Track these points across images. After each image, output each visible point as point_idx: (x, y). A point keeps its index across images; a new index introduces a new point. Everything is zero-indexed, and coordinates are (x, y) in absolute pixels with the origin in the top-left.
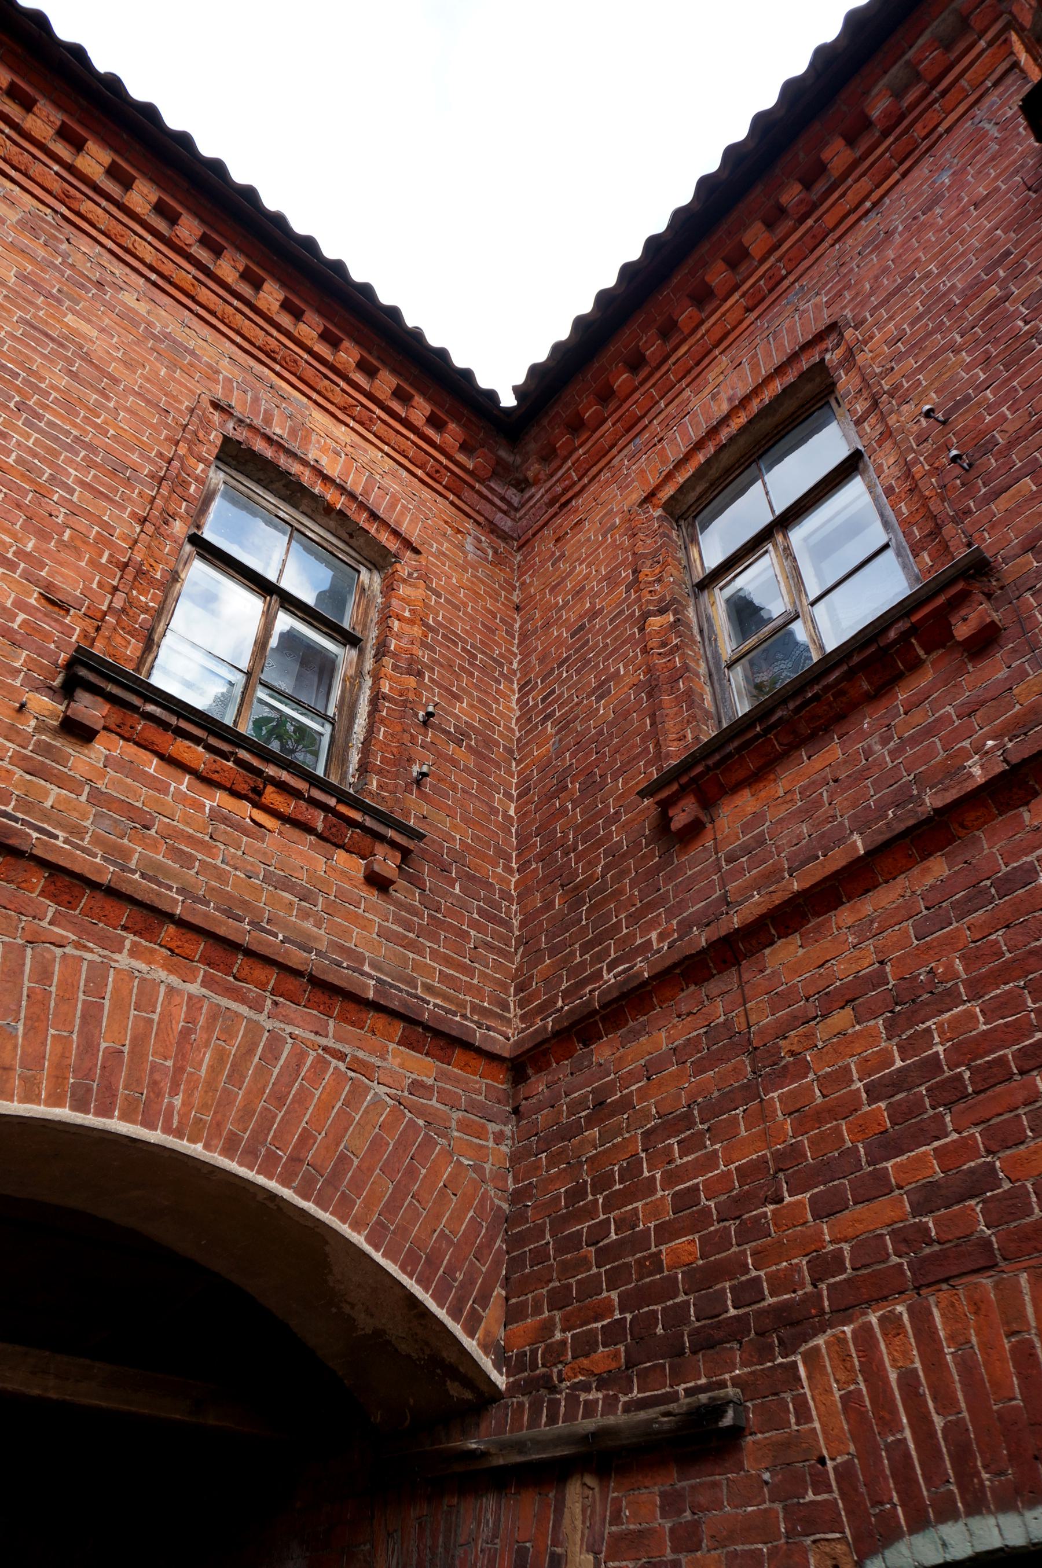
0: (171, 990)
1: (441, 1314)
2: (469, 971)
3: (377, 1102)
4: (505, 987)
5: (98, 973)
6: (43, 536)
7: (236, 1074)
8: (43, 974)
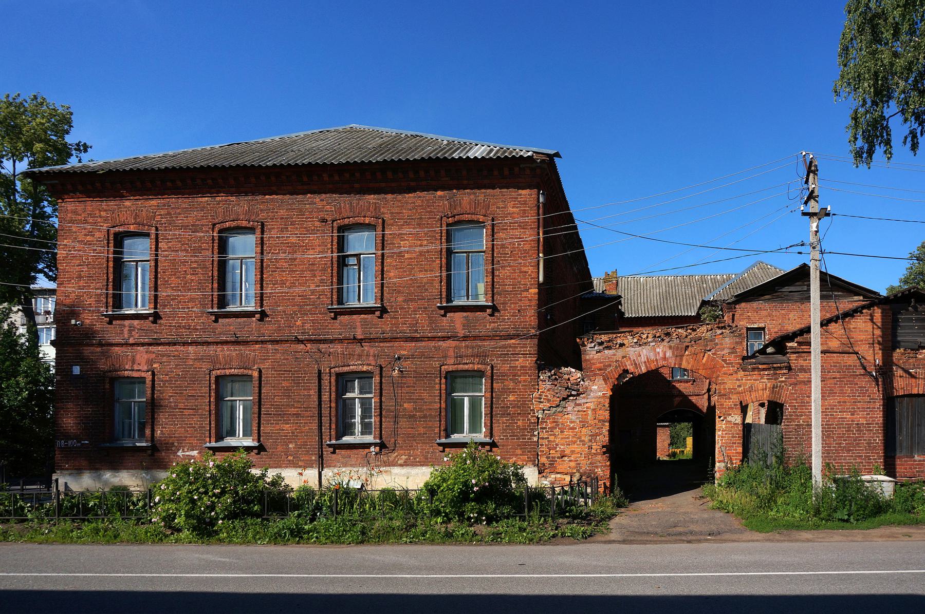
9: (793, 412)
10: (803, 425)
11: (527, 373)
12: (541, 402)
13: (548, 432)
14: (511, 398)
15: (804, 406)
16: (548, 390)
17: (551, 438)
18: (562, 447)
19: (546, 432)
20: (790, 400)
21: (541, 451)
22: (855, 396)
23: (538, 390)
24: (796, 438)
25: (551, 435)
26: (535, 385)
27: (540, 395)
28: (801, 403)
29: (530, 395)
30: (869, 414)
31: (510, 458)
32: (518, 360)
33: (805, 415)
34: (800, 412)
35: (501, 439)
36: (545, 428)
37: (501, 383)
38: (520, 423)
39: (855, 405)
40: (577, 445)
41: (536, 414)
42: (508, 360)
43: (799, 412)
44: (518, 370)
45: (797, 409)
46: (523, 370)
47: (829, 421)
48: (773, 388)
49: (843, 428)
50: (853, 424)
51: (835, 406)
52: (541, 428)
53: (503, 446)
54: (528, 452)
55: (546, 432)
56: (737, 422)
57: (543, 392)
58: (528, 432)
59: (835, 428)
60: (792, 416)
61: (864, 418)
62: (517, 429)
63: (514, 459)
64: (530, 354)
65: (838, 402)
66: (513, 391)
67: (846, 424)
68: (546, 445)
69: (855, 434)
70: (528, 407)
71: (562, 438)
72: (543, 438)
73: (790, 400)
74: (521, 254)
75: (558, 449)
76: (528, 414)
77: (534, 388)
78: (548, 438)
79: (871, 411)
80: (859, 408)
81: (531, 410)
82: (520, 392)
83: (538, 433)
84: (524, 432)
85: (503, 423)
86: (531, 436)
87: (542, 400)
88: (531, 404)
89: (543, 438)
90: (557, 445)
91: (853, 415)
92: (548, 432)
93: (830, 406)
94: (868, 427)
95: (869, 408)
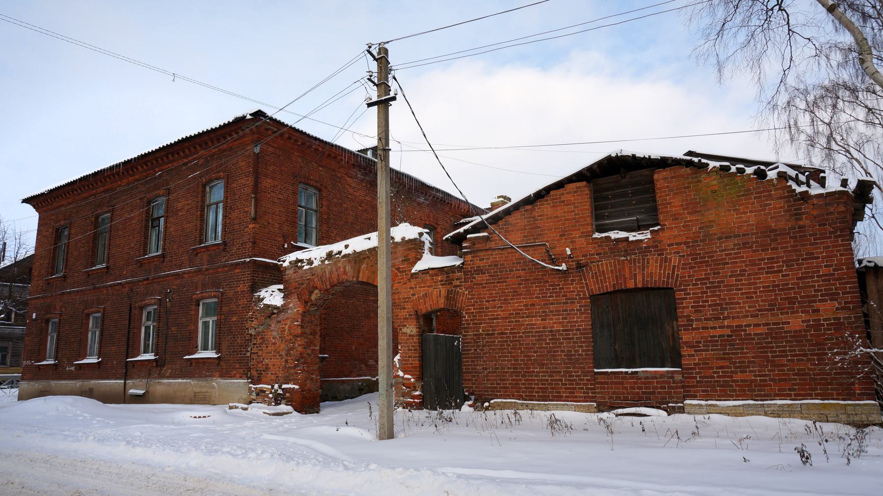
9: (471, 320)
12: (252, 321)
20: (467, 306)
22: (546, 297)
28: (480, 309)
29: (246, 315)
30: (566, 318)
31: (231, 371)
32: (239, 286)
33: (485, 323)
34: (479, 320)
38: (239, 341)
39: (547, 308)
41: (250, 332)
44: (239, 294)
45: (475, 316)
46: (243, 294)
47: (514, 329)
48: (448, 294)
49: (532, 336)
50: (545, 331)
51: (521, 310)
56: (412, 334)
59: (522, 337)
61: (560, 323)
62: (236, 346)
64: (248, 280)
65: (525, 306)
67: (536, 332)
69: (548, 344)
71: (267, 353)
73: (467, 306)
74: (246, 197)
78: (257, 353)
79: (568, 314)
80: (552, 312)
83: (251, 349)
85: (229, 341)
89: (254, 353)
90: (263, 359)
91: (545, 320)
93: (514, 310)
94: (513, 337)
95: (566, 310)
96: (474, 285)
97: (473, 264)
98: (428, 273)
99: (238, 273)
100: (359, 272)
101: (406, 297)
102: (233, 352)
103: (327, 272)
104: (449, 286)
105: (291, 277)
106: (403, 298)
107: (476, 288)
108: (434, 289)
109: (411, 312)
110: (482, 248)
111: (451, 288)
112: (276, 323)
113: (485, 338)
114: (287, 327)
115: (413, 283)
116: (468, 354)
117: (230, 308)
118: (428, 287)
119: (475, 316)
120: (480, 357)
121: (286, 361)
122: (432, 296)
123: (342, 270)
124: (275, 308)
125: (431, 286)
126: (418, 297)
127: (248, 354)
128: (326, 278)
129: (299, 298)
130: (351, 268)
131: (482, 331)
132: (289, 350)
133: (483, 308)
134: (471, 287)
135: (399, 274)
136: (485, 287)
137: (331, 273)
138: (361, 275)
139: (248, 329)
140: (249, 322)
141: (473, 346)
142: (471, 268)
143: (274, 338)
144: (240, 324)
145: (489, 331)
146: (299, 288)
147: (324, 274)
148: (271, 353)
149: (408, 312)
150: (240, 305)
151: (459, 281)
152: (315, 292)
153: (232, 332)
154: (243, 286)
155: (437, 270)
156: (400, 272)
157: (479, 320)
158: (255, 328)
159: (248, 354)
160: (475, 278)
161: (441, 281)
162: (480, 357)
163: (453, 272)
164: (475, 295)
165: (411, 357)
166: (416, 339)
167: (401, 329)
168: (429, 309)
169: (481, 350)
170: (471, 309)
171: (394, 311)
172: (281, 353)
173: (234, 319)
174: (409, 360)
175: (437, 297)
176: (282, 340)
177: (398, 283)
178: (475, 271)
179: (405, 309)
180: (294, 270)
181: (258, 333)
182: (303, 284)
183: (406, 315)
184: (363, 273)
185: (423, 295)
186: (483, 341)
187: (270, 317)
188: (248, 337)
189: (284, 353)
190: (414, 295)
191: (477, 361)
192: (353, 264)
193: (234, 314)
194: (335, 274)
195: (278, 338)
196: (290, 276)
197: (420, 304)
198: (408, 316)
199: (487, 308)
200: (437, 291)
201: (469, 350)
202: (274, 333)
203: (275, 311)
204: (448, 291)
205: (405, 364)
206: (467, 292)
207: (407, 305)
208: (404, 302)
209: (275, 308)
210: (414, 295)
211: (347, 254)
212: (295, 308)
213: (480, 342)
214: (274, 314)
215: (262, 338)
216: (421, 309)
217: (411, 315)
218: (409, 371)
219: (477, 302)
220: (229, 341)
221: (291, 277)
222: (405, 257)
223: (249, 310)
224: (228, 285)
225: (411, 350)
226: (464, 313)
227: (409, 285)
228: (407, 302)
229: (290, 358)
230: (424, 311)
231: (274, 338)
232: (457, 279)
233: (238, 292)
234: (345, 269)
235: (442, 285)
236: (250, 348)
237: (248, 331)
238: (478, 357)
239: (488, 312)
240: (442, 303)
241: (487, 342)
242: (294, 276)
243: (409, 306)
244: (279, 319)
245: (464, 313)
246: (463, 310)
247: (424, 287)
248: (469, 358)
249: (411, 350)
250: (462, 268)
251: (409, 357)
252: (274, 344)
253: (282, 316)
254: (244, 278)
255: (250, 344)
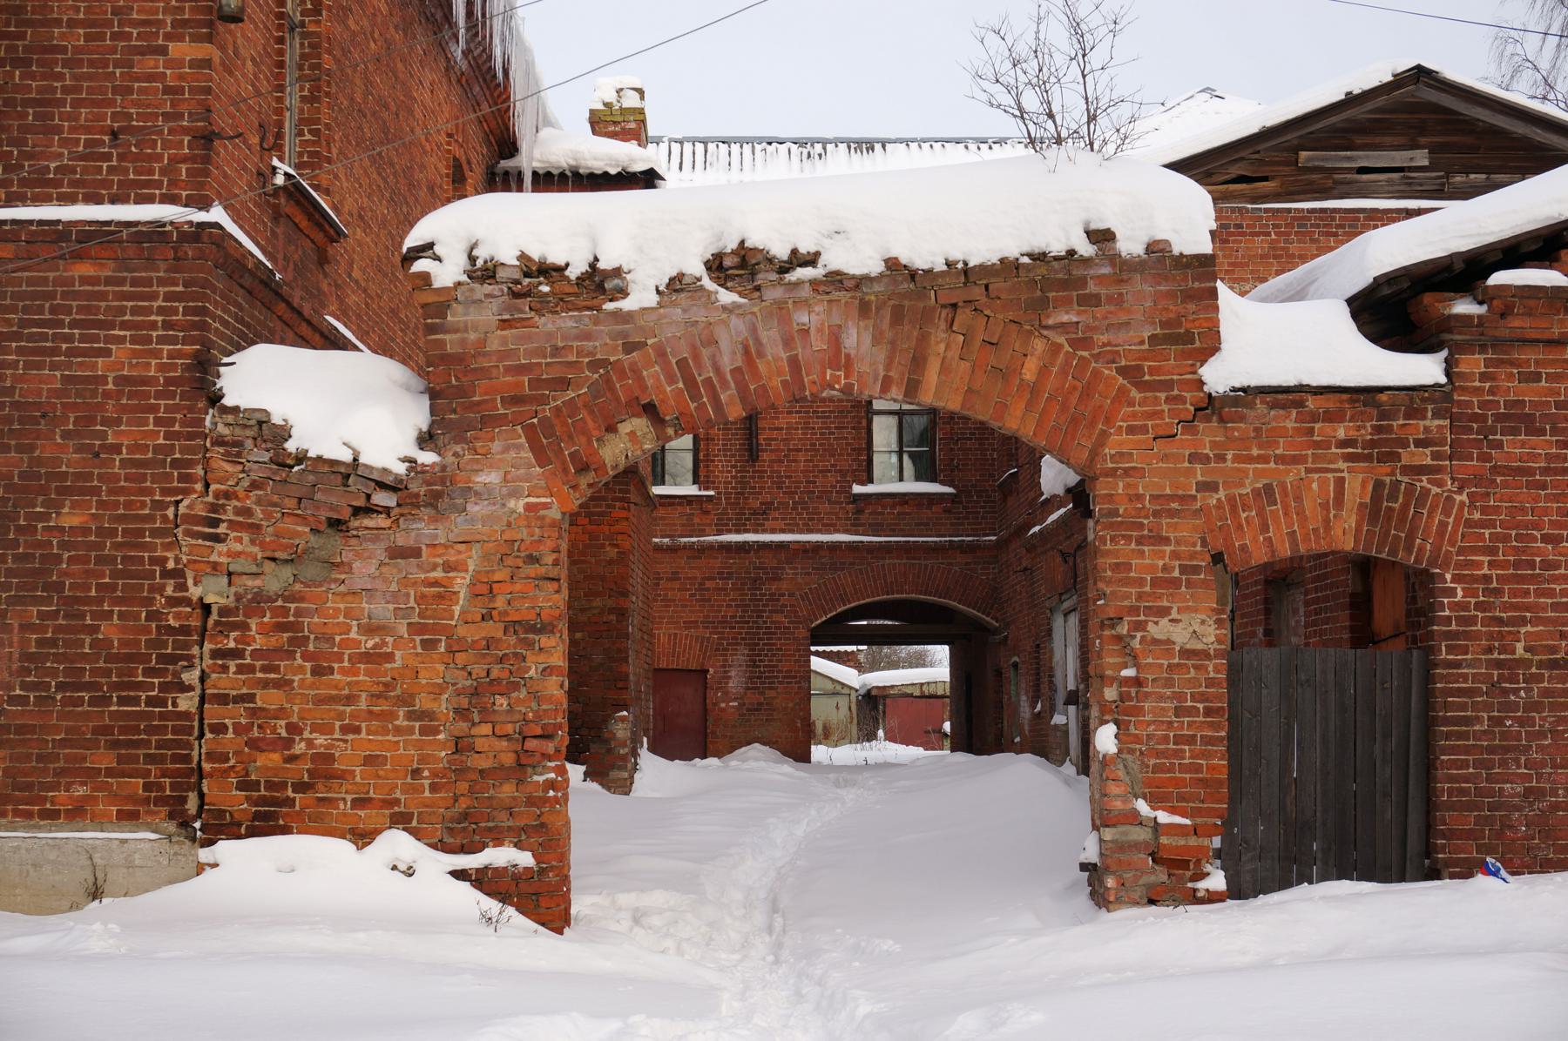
0: (899, 564)
1: (979, 614)
2: (980, 524)
3: (956, 572)
4: (994, 523)
5: (883, 566)
6: (833, 455)
7: (919, 577)
8: (873, 571)
9: (1478, 606)
10: (1526, 663)
11: (154, 409)
12: (217, 539)
13: (251, 669)
14: (70, 518)
15: (1533, 579)
16: (254, 485)
17: (268, 699)
18: (320, 740)
19: (241, 669)
20: (1461, 551)
21: (211, 757)
23: (207, 486)
24: (1499, 722)
25: (265, 684)
26: (191, 464)
27: (214, 508)
28: (1517, 564)
29: (162, 506)
31: (54, 787)
32: (108, 353)
33: (1535, 621)
34: (1515, 607)
35: (13, 700)
36: (236, 654)
37: (20, 449)
40: (398, 731)
41: (195, 592)
42: (54, 351)
43: (1506, 607)
44: (106, 394)
46: (131, 396)
52: (215, 654)
53: (21, 729)
54: (150, 759)
55: (241, 669)
57: (228, 495)
58: (149, 672)
60: (1472, 620)
63: (81, 791)
64: (167, 325)
66: (77, 488)
68: (238, 729)
70: (153, 561)
71: (320, 701)
72: (223, 699)
73: (1461, 551)
75: (299, 748)
76: (152, 589)
77: (184, 478)
78: (251, 698)
81: (167, 574)
82: (110, 492)
83: (202, 679)
84: (132, 672)
86: (164, 687)
87: (222, 529)
88: (167, 547)
89: (223, 699)
92: (251, 669)
96: (1495, 470)
97: (1492, 391)
98: (1300, 404)
99: (85, 280)
100: (918, 362)
101: (1168, 491)
102: (61, 687)
103: (724, 344)
104: (1385, 468)
105: (483, 342)
106: (1154, 498)
107: (1505, 485)
108: (1308, 471)
109: (1193, 556)
110: (1534, 335)
111: (1393, 474)
112: (382, 556)
113: (1539, 678)
114: (461, 583)
115: (1208, 435)
116: (1463, 736)
117: (39, 461)
118: (1280, 459)
119: (1497, 592)
120: (1515, 749)
121: (461, 745)
122: (1298, 499)
123: (818, 343)
124: (382, 486)
125: (1296, 460)
126: (1231, 499)
127: (187, 703)
128: (717, 369)
129: (536, 448)
130: (877, 340)
131: (1527, 649)
132: (476, 699)
133: (1532, 565)
134: (1478, 480)
135: (1135, 393)
136: (1544, 486)
137: (750, 353)
138: (932, 375)
139: (178, 574)
140: (186, 541)
141: (1488, 707)
142: (1482, 405)
143: (370, 630)
144: (117, 546)
145: (1553, 650)
146: (543, 400)
147: (705, 353)
148: (350, 699)
149: (1175, 555)
150: (117, 449)
151: (1428, 451)
152: (625, 428)
153: (59, 587)
154: (135, 353)
155: (1345, 396)
156: (1143, 386)
157: (1515, 607)
158: (230, 574)
159: (187, 703)
160: (1499, 445)
161: (1343, 444)
162: (1515, 749)
163: (1414, 413)
164: (1497, 510)
165: (1191, 740)
166: (1215, 669)
167: (1140, 626)
168: (1285, 551)
169: (1521, 722)
170: (1479, 565)
171: (1108, 547)
172: (423, 702)
173: (70, 518)
174: (1178, 754)
175: (1325, 506)
176: (429, 645)
177: (1131, 430)
178: (1499, 418)
179: (1167, 541)
180: (508, 309)
181: (258, 602)
182: (564, 384)
183: (1165, 568)
184: (945, 369)
185: (1256, 493)
186: (1528, 690)
187: (336, 524)
188: (177, 616)
189: (443, 706)
190: (1208, 487)
191: (1503, 763)
192: (887, 321)
193: (63, 491)
194: (774, 349)
195: (403, 630)
196: (472, 336)
197: (1240, 527)
198: (1176, 574)
199: (1548, 565)
200: (1323, 483)
201: (1467, 721)
202: (381, 610)
203: (382, 499)
204: (1379, 485)
205: (1157, 769)
206: (1464, 497)
207: (1175, 527)
208: (1156, 514)
209: (382, 486)
210: (1208, 487)
211: (853, 277)
212: (515, 494)
213: (1516, 691)
214: (369, 510)
215: (281, 627)
216: (1244, 548)
217: (1196, 570)
218: (1181, 798)
219: (1506, 538)
220: (26, 627)
221: (483, 342)
222: (1163, 325)
223: (184, 478)
224: (16, 336)
225: (1192, 711)
226: (1448, 577)
227: (1184, 444)
228: (1172, 514)
229: (486, 729)
230: (1260, 556)
231: (370, 630)
232: (1419, 443)
233: (103, 380)
234: (835, 338)
235: (1349, 458)
236: (197, 673)
237: (183, 587)
238: (1506, 750)
239: (1555, 579)
240: (1346, 534)
241: (1546, 693)
242: (504, 341)
243: (1185, 534)
244: (401, 540)
245: (1448, 577)
246: (1445, 566)
247: (1263, 459)
248: (1467, 750)
249: (1192, 711)
250: (1447, 397)
251: (1178, 740)
252: (376, 658)
253: (421, 530)
254: (136, 311)
255: (195, 650)
